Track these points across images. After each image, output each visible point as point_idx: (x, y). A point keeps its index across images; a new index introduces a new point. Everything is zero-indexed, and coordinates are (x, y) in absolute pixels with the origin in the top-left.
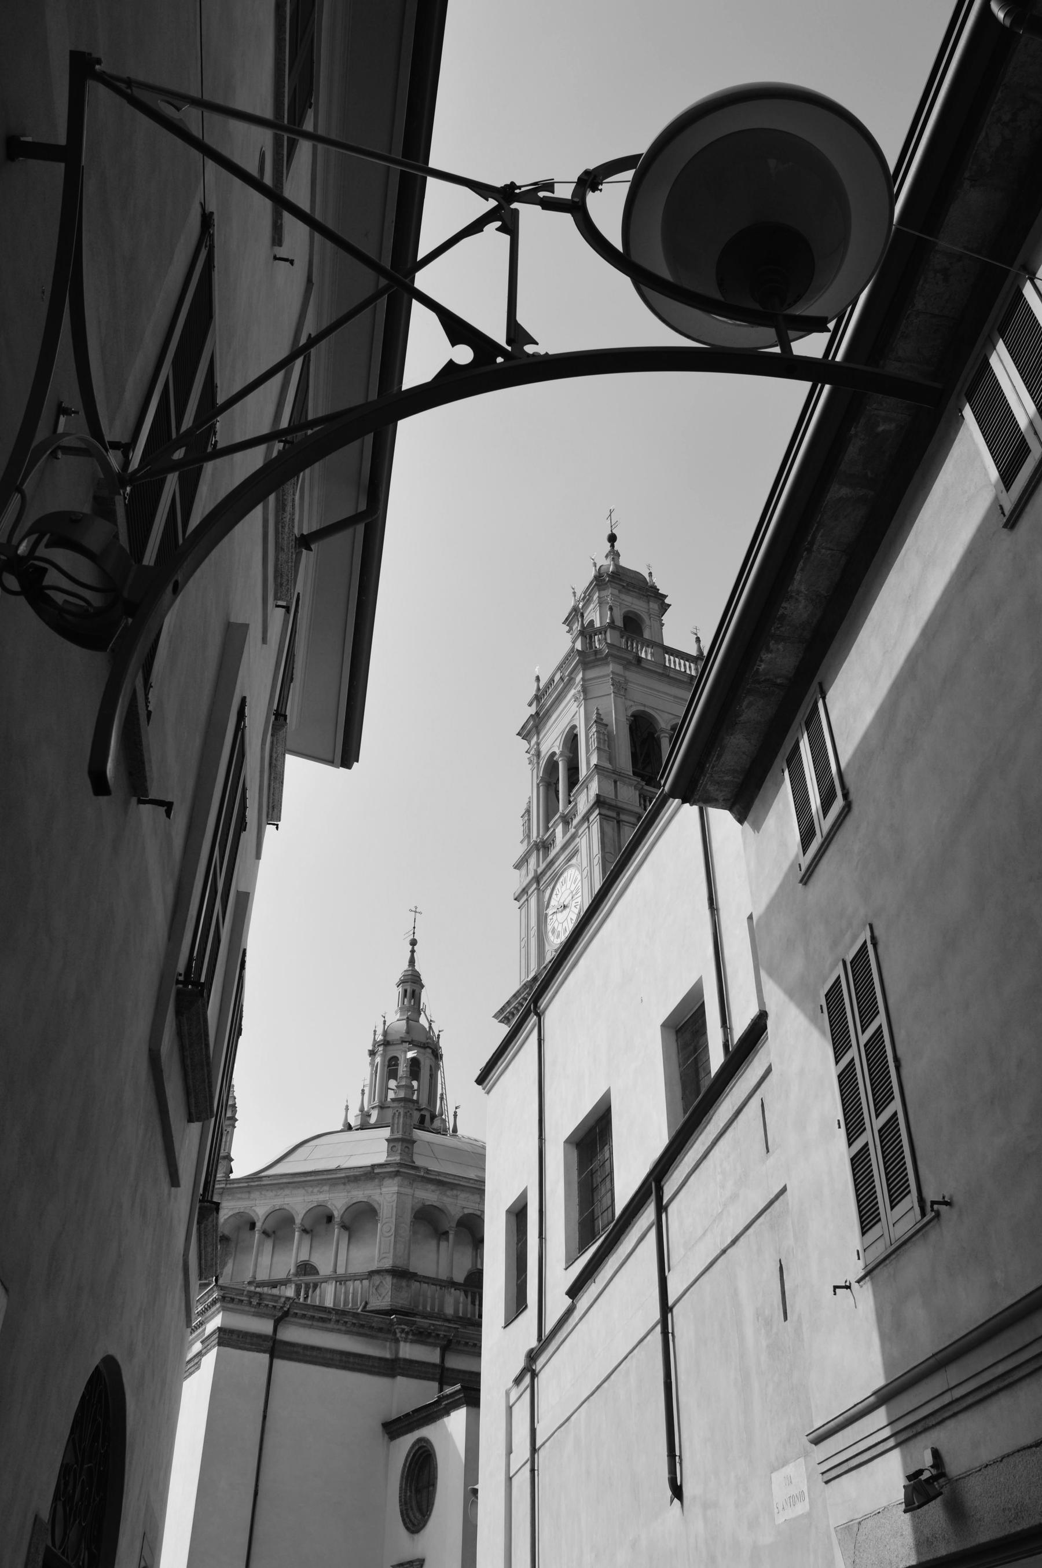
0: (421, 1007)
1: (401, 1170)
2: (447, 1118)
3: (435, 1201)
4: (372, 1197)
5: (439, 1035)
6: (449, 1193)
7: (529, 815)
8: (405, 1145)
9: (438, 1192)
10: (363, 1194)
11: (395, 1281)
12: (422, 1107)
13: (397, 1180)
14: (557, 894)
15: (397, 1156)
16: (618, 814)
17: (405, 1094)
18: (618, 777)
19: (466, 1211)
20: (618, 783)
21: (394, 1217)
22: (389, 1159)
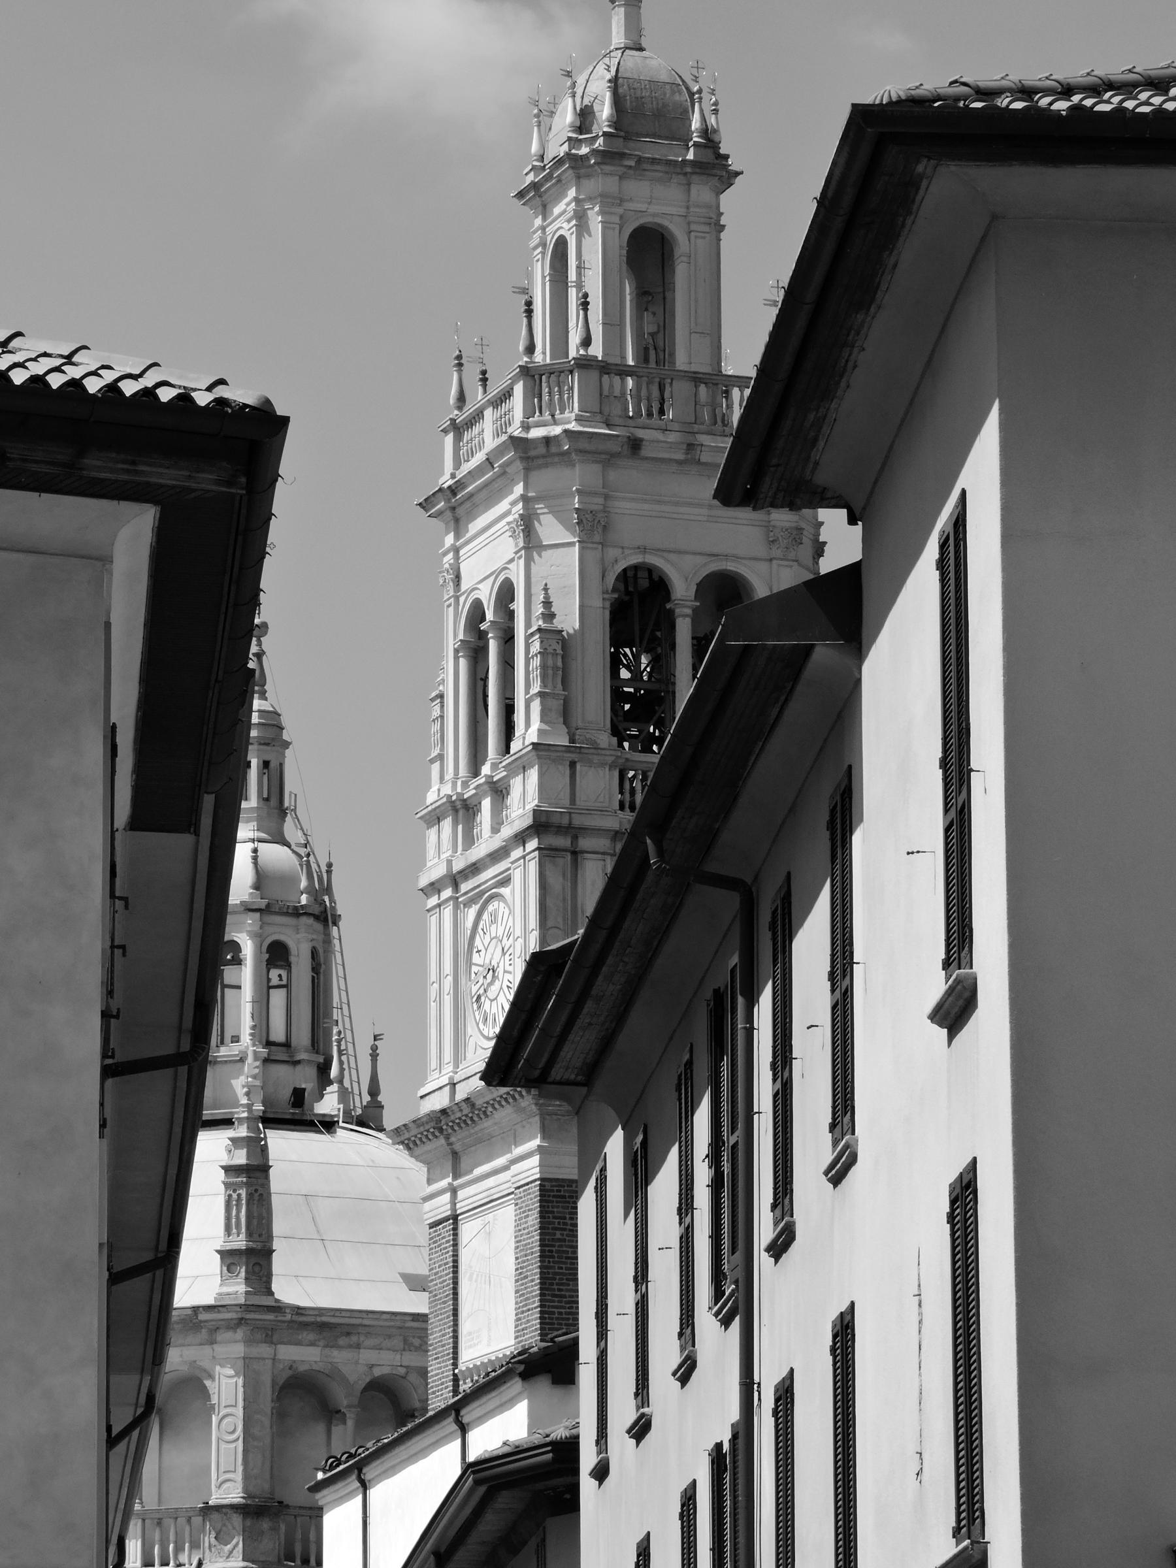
0: (286, 804)
1: (248, 1316)
2: (355, 1085)
3: (316, 1362)
4: (198, 1363)
5: (330, 865)
6: (342, 1341)
7: (442, 707)
8: (253, 1260)
9: (321, 1343)
10: (181, 1356)
11: (248, 1523)
12: (298, 1058)
13: (240, 1334)
14: (479, 951)
15: (239, 1284)
16: (575, 838)
17: (248, 1157)
18: (577, 755)
19: (377, 1372)
20: (578, 767)
21: (241, 1403)
22: (225, 1289)
